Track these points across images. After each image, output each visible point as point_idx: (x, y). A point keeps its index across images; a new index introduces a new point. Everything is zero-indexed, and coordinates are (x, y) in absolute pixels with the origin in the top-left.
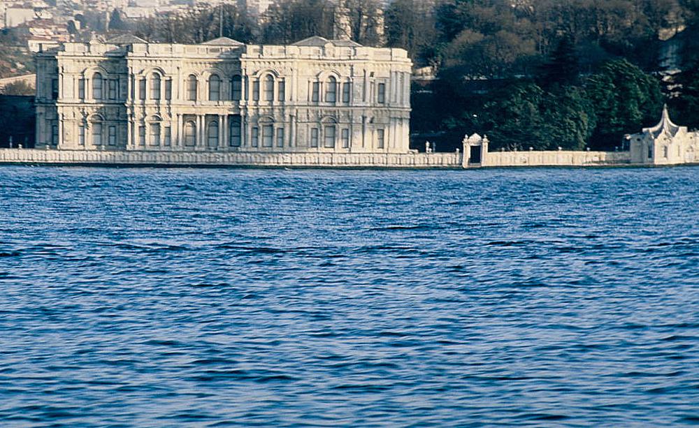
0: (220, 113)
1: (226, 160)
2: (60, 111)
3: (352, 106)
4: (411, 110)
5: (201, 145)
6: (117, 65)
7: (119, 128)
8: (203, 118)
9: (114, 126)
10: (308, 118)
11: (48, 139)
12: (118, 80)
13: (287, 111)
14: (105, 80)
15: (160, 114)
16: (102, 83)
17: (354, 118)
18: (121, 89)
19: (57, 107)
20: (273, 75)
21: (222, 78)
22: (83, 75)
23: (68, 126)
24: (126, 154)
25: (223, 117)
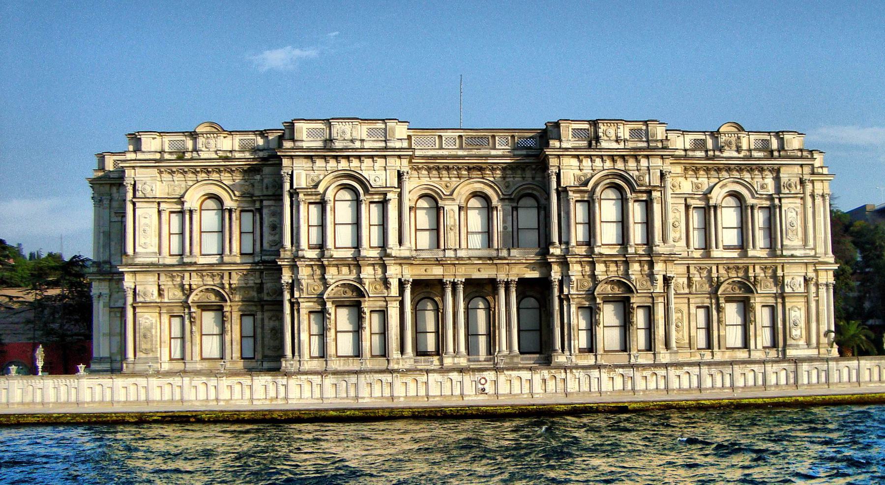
0: (502, 277)
1: (538, 388)
2: (128, 282)
3: (782, 256)
4: (836, 267)
5: (456, 351)
6: (258, 177)
7: (263, 319)
8: (461, 288)
9: (253, 315)
10: (690, 286)
11: (115, 350)
12: (260, 211)
13: (659, 267)
14: (230, 211)
15: (360, 281)
16: (223, 219)
17: (787, 280)
18: (264, 229)
19: (122, 273)
20: (617, 181)
21: (495, 201)
22: (183, 203)
23: (147, 318)
24: (282, 380)
25: (507, 284)
